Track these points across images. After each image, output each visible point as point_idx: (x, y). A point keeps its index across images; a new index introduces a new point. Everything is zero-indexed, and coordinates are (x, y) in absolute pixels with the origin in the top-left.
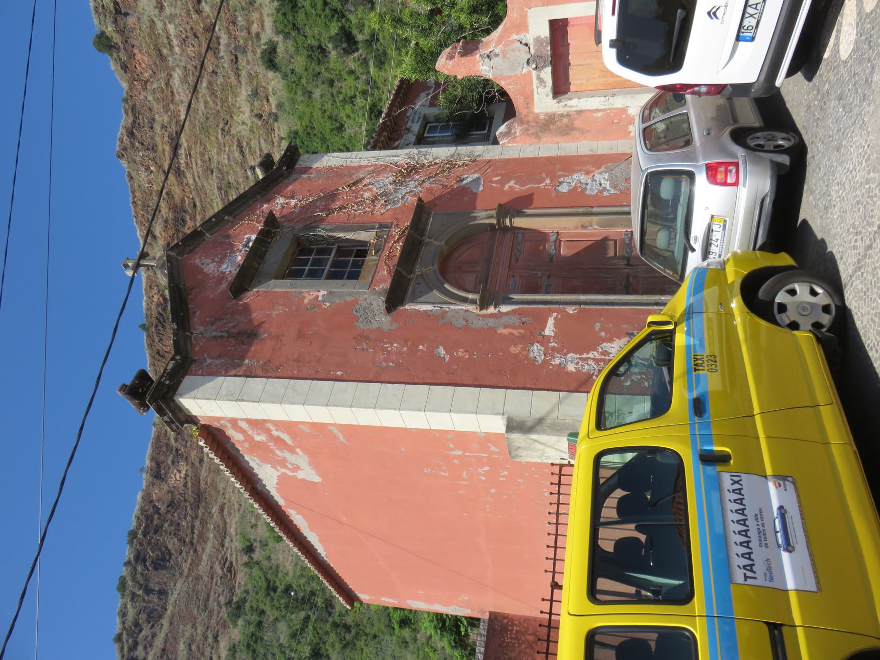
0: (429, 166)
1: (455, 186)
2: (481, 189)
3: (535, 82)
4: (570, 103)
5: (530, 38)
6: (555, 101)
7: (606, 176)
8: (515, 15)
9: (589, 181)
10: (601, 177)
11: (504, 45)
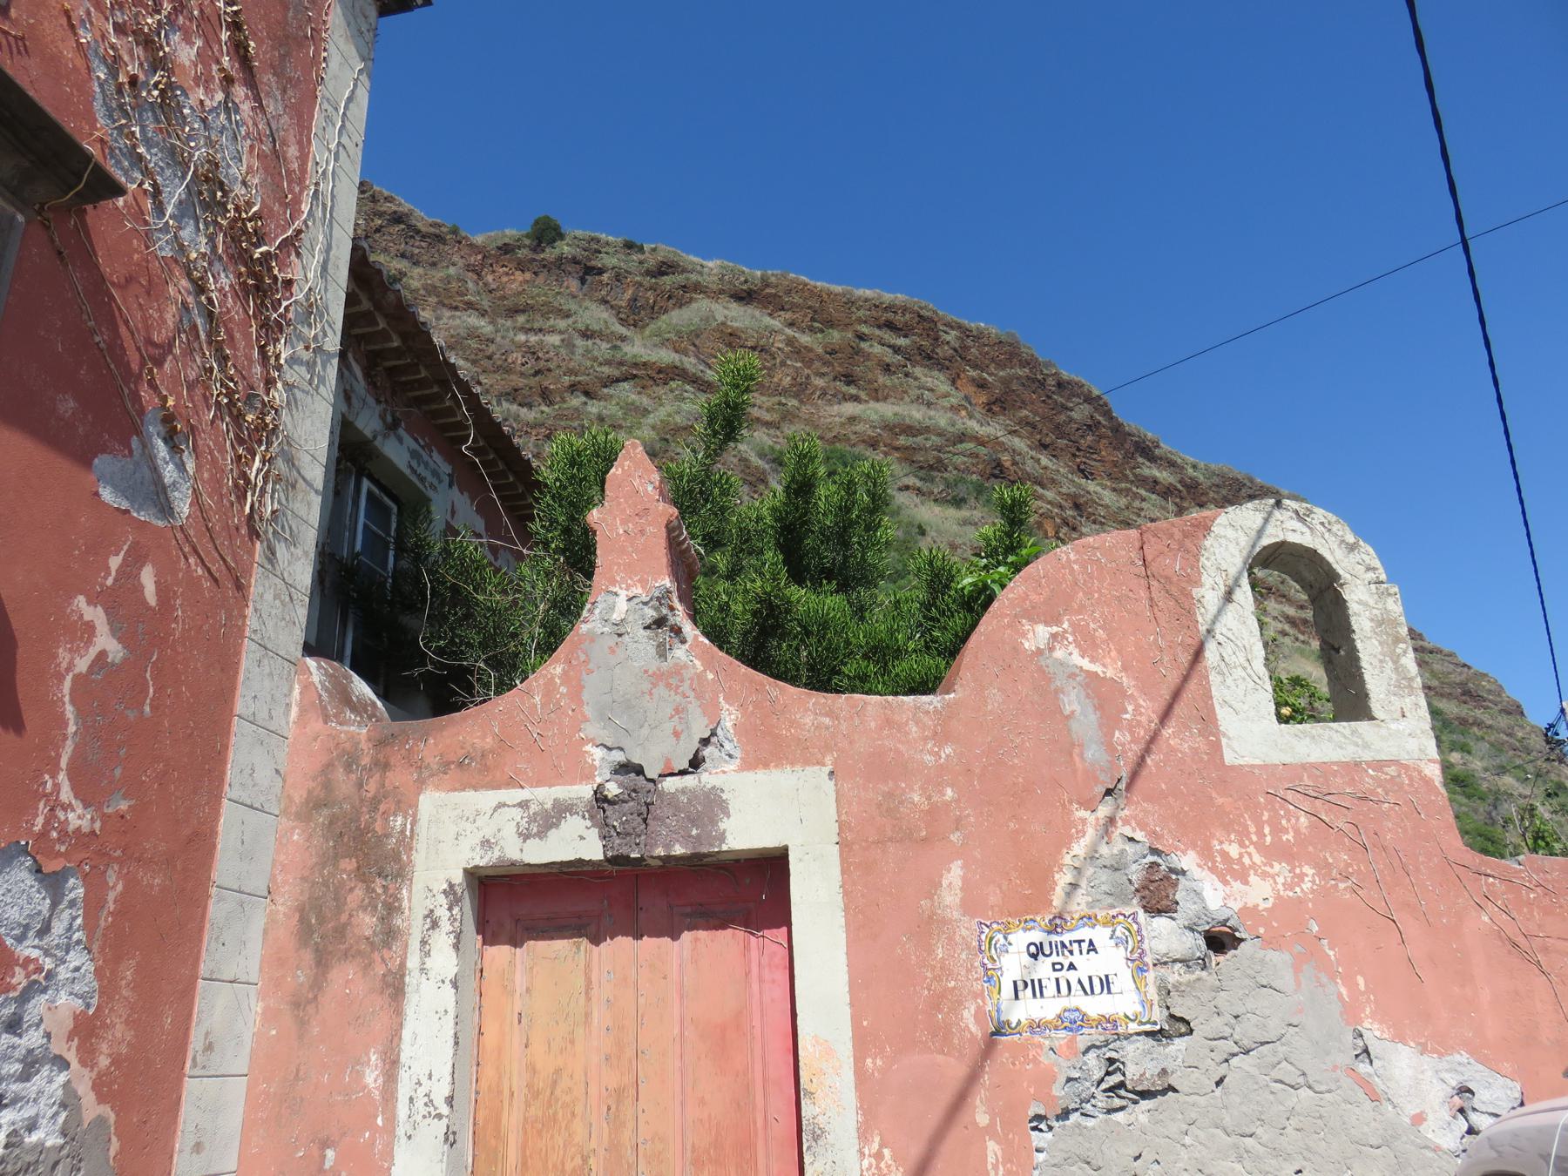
0: (262, 349)
1: (145, 393)
2: (107, 495)
3: (545, 795)
4: (442, 941)
5: (720, 774)
6: (458, 878)
7: (47, 1136)
8: (808, 720)
9: (32, 1039)
10: (45, 1108)
11: (700, 677)
